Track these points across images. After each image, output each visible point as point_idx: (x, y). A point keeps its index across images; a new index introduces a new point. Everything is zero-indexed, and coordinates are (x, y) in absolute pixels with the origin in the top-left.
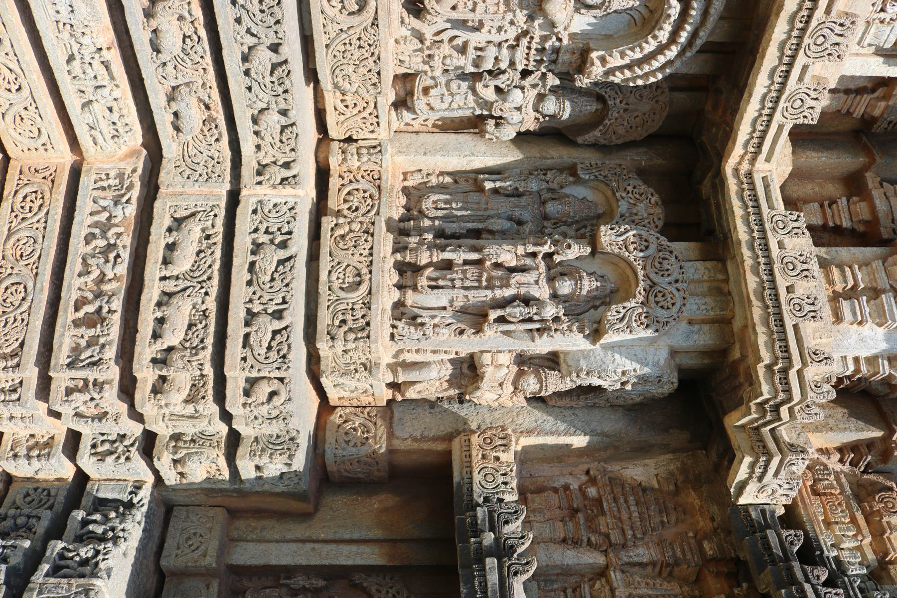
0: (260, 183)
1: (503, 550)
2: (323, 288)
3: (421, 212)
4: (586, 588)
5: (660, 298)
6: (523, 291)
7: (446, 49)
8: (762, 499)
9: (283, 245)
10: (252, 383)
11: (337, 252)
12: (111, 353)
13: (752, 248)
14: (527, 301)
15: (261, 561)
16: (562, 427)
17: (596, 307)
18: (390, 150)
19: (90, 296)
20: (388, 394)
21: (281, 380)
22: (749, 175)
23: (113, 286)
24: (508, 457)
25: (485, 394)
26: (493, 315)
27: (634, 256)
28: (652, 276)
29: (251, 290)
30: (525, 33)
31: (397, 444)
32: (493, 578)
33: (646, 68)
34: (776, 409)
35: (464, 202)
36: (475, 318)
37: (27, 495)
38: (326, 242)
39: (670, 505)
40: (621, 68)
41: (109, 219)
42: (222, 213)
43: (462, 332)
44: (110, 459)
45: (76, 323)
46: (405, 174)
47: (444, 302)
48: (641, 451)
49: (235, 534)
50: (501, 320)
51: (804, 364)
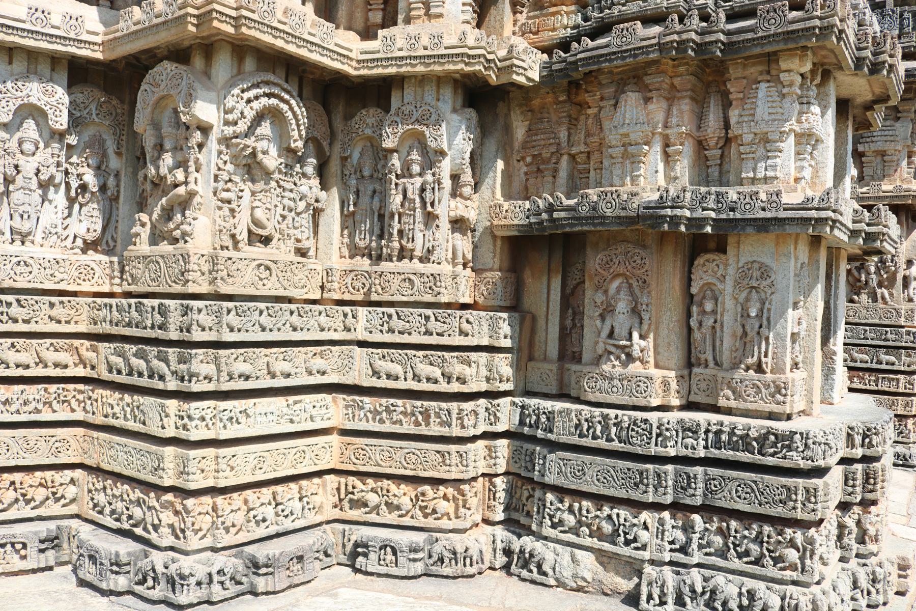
0: (355, 329)
1: (550, 209)
2: (412, 299)
3: (366, 248)
4: (580, 167)
5: (425, 118)
6: (417, 192)
7: (283, 226)
8: (537, 68)
9: (390, 316)
10: (463, 333)
11: (392, 292)
12: (444, 405)
13: (401, 66)
14: (423, 190)
15: (557, 342)
16: (491, 174)
17: (427, 152)
18: (328, 264)
19: (413, 418)
20: (469, 270)
21: (461, 317)
22: (358, 61)
23: (408, 406)
24: (506, 205)
25: (472, 215)
26: (429, 209)
27: (401, 129)
28: (412, 120)
29: (413, 333)
30: (277, 182)
31: (496, 266)
32: (563, 214)
33: (300, 117)
34: (488, 61)
35: (361, 222)
36: (430, 218)
37: (516, 462)
38: (386, 297)
39: (539, 116)
40: (299, 131)
41: (370, 412)
42: (370, 350)
43: (438, 226)
44: (498, 414)
45: (428, 424)
46: (341, 257)
47: (421, 235)
48: (508, 129)
49: (542, 357)
50: (432, 204)
51: (466, 46)
